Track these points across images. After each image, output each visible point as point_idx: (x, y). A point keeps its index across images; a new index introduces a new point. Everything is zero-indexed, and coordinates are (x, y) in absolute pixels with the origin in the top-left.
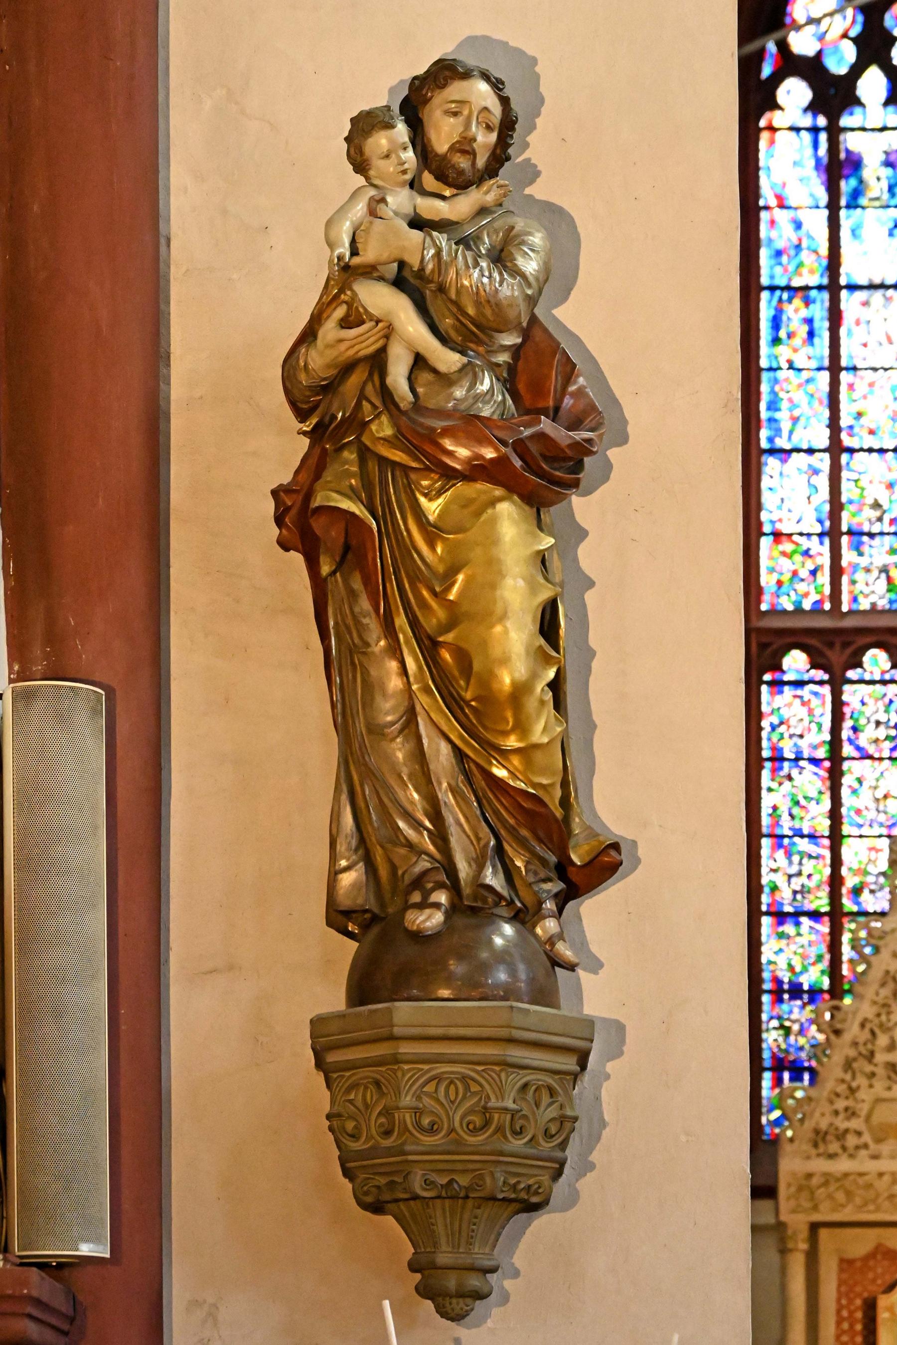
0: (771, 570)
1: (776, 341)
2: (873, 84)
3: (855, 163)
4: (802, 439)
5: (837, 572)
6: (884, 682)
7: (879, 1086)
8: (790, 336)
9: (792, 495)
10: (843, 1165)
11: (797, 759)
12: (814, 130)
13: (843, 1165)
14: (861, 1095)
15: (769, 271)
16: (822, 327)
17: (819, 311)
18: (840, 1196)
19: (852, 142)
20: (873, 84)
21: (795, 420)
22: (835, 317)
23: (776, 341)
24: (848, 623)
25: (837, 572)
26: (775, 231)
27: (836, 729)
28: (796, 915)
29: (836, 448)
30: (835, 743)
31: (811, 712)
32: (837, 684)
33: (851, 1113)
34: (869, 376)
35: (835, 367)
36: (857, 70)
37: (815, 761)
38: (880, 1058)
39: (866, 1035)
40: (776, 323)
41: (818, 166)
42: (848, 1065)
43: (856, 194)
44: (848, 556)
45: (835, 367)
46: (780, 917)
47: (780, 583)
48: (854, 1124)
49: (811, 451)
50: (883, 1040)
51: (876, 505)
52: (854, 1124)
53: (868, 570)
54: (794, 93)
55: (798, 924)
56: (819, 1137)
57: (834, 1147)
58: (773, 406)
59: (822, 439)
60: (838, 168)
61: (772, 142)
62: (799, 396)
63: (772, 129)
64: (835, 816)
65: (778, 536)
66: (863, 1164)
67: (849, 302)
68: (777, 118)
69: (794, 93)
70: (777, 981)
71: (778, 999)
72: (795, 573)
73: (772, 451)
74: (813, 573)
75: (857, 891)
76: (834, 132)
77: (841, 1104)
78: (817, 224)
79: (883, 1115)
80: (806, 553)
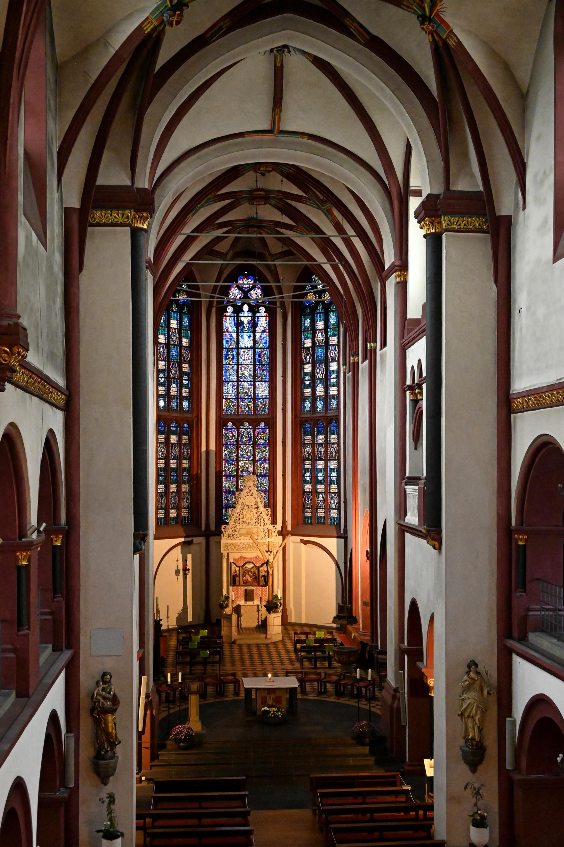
0: (225, 406)
1: (226, 359)
2: (246, 308)
3: (242, 323)
4: (231, 379)
5: (238, 406)
6: (248, 429)
7: (241, 525)
8: (229, 358)
9: (229, 390)
10: (233, 541)
11: (230, 444)
12: (234, 316)
13: (233, 541)
14: (237, 527)
15: (225, 345)
16: (235, 356)
17: (235, 353)
18: (233, 547)
19: (242, 319)
20: (246, 308)
21: (230, 375)
22: (238, 354)
23: (226, 359)
24: (241, 417)
25: (238, 406)
26: (227, 336)
27: (238, 438)
28: (230, 477)
29: (238, 381)
30: (237, 441)
31: (233, 435)
32: (238, 429)
33: (235, 531)
34: (245, 366)
35: (238, 364)
36: (243, 305)
37: (233, 445)
38: (241, 520)
39: (238, 515)
40: (226, 355)
41: (234, 324)
42: (235, 521)
43: (242, 329)
44: (241, 403)
45: (238, 364)
46: (227, 477)
47: (227, 408)
48: (236, 533)
49: (233, 381)
50: (241, 516)
51: (246, 392)
52: (236, 533)
53: (244, 406)
54: (230, 309)
55: (230, 478)
56: (229, 536)
57: (232, 537)
58: (226, 372)
59: (235, 379)
60: (239, 324)
61: (226, 319)
62: (231, 370)
63: (226, 316)
64: (237, 456)
65: (227, 399)
66: (237, 541)
67: (241, 352)
68: (228, 314)
69: (230, 309)
70: (226, 490)
71: (226, 494)
72: (230, 406)
73: (226, 381)
74: (233, 406)
75: (242, 471)
76: (238, 317)
77: (233, 529)
78: (234, 335)
79: (241, 531)
80: (232, 402)
